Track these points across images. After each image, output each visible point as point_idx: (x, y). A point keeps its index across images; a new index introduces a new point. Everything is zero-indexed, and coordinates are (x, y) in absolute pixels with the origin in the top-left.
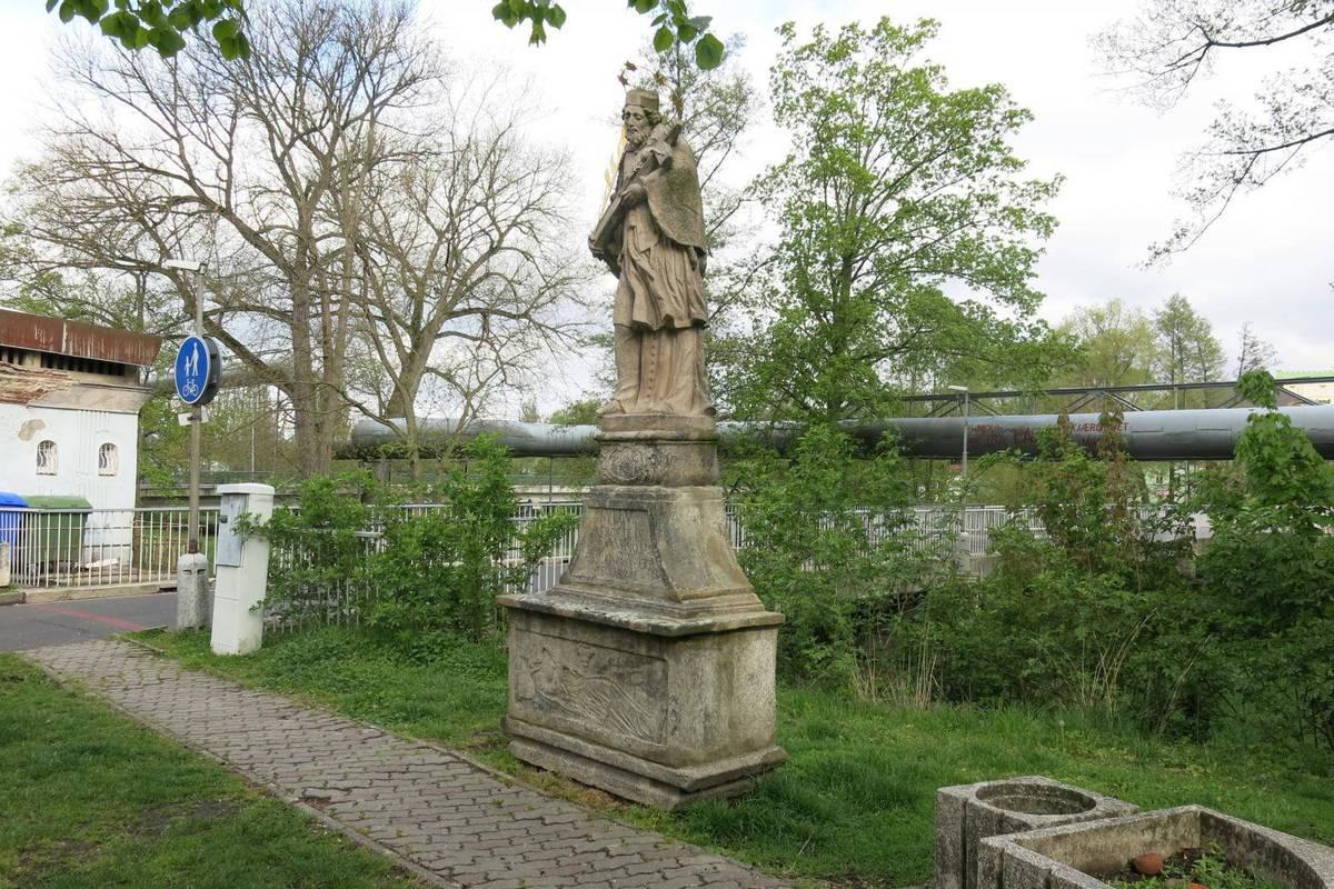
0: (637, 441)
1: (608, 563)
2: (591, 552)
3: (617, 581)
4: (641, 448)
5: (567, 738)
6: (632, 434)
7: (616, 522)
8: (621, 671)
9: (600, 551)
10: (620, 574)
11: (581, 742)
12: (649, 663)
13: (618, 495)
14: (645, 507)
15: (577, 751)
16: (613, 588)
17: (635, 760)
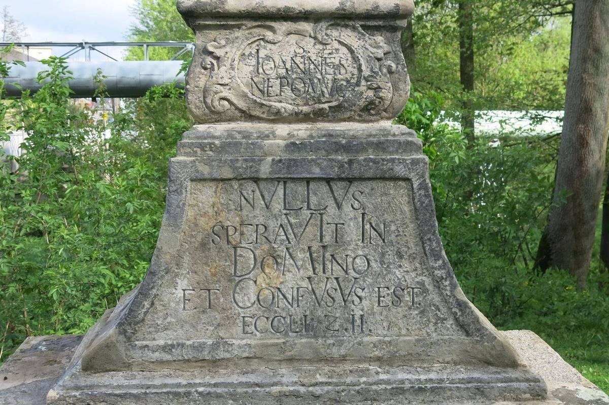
1: (266, 306)
3: (301, 343)
4: (349, 36)
9: (235, 281)
10: (309, 326)
13: (292, 146)
14: (400, 170)
16: (291, 360)
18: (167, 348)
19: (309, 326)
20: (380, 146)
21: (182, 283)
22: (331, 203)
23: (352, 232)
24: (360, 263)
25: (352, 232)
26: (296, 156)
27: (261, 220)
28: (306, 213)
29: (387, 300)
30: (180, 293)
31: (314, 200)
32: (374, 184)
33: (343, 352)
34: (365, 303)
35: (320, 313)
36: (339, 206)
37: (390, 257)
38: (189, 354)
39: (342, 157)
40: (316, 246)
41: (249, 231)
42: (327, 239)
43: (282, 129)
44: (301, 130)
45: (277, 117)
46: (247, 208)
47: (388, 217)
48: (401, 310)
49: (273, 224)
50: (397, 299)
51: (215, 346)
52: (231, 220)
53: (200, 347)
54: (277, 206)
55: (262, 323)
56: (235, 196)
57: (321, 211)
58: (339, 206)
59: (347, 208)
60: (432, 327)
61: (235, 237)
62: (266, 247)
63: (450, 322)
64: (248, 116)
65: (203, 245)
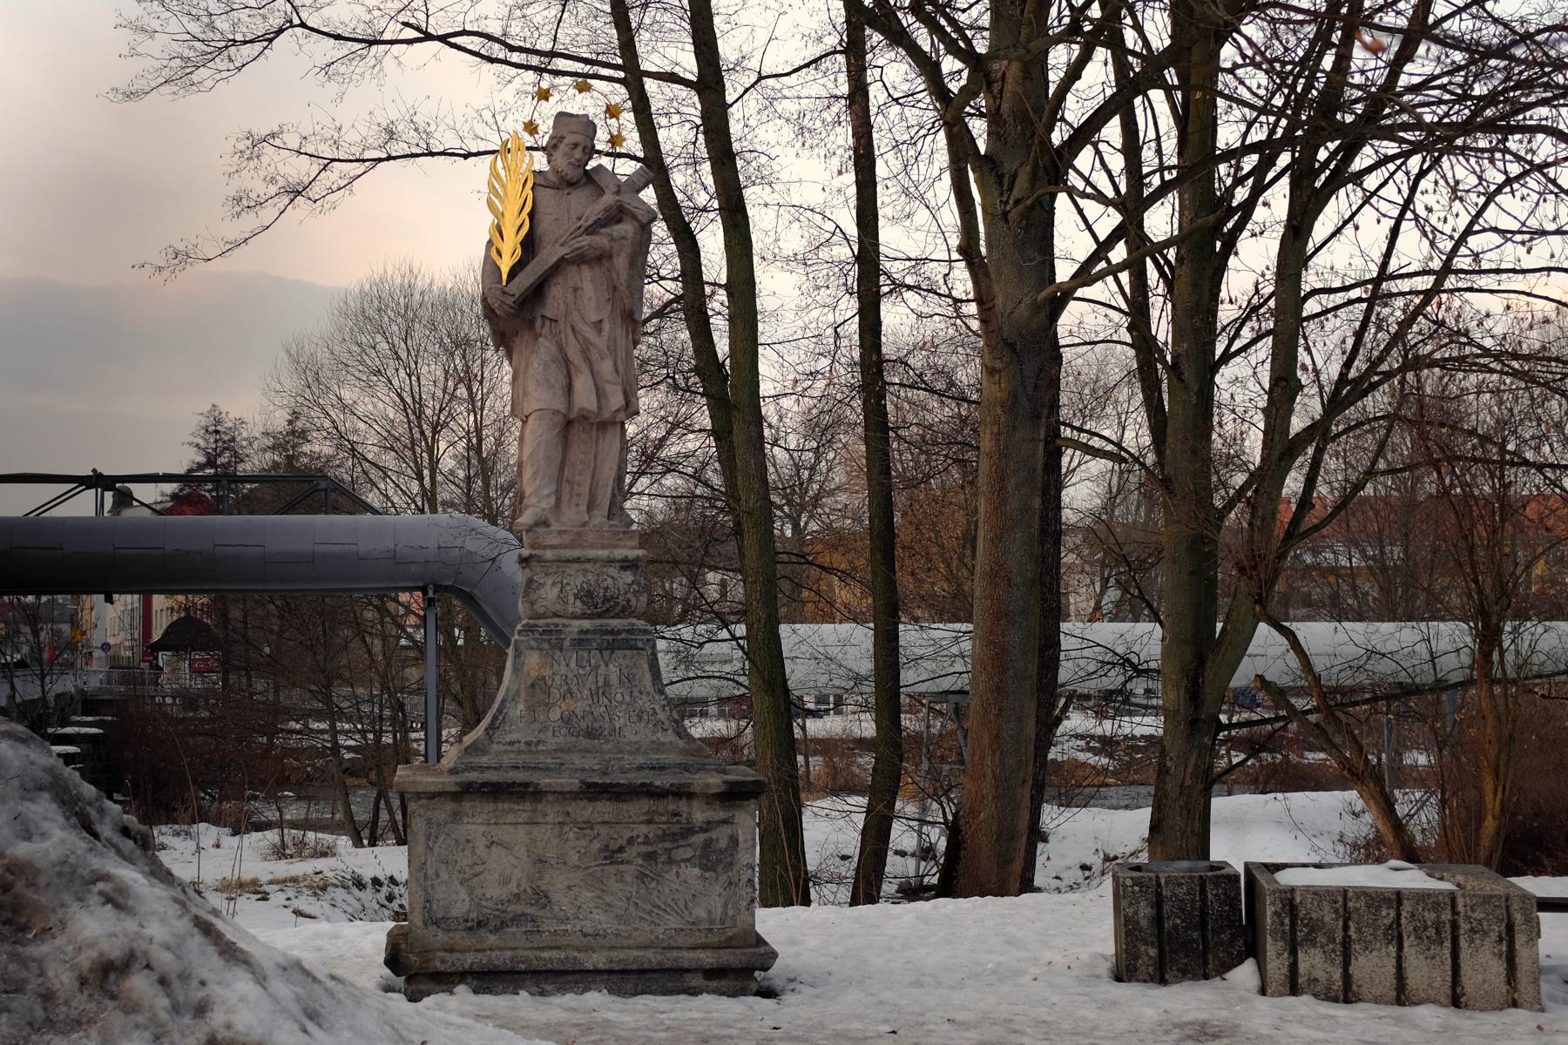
0: (610, 561)
1: (566, 720)
2: (531, 709)
3: (584, 742)
4: (612, 571)
5: (545, 955)
6: (604, 553)
7: (579, 666)
8: (650, 849)
9: (548, 706)
10: (590, 733)
11: (576, 954)
12: (706, 831)
13: (582, 632)
14: (640, 644)
15: (569, 967)
17: (685, 954)
18: (512, 743)
19: (590, 733)
20: (630, 632)
21: (521, 707)
22: (602, 664)
23: (614, 679)
24: (619, 697)
25: (614, 679)
26: (583, 637)
27: (564, 672)
28: (588, 668)
29: (634, 719)
30: (518, 712)
31: (593, 661)
32: (626, 652)
33: (609, 746)
34: (622, 720)
35: (596, 725)
36: (607, 665)
37: (636, 693)
38: (523, 747)
39: (610, 638)
40: (593, 688)
41: (557, 678)
42: (600, 684)
43: (576, 623)
44: (586, 624)
45: (574, 617)
46: (556, 666)
47: (635, 671)
48: (643, 724)
49: (570, 675)
50: (640, 718)
51: (539, 742)
52: (547, 672)
53: (528, 744)
54: (573, 665)
55: (563, 731)
56: (549, 659)
57: (597, 667)
58: (607, 665)
59: (611, 666)
60: (659, 735)
61: (549, 683)
62: (565, 688)
63: (670, 732)
64: (556, 615)
65: (533, 686)
